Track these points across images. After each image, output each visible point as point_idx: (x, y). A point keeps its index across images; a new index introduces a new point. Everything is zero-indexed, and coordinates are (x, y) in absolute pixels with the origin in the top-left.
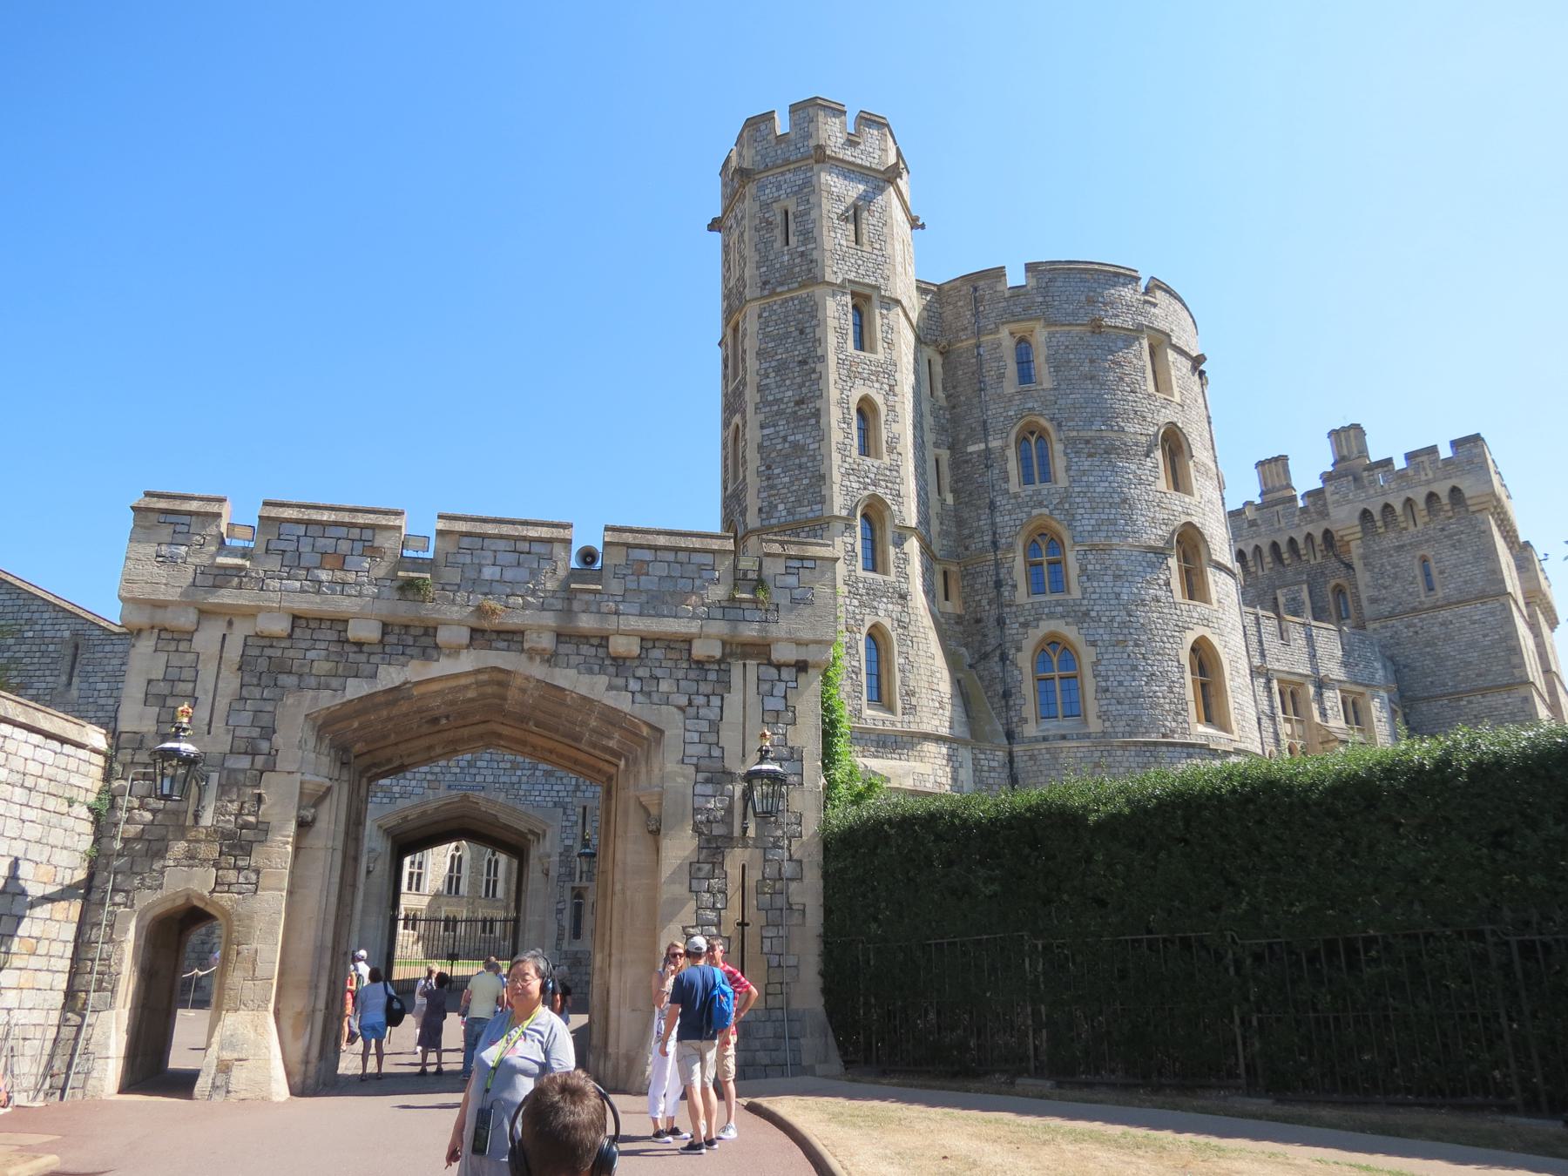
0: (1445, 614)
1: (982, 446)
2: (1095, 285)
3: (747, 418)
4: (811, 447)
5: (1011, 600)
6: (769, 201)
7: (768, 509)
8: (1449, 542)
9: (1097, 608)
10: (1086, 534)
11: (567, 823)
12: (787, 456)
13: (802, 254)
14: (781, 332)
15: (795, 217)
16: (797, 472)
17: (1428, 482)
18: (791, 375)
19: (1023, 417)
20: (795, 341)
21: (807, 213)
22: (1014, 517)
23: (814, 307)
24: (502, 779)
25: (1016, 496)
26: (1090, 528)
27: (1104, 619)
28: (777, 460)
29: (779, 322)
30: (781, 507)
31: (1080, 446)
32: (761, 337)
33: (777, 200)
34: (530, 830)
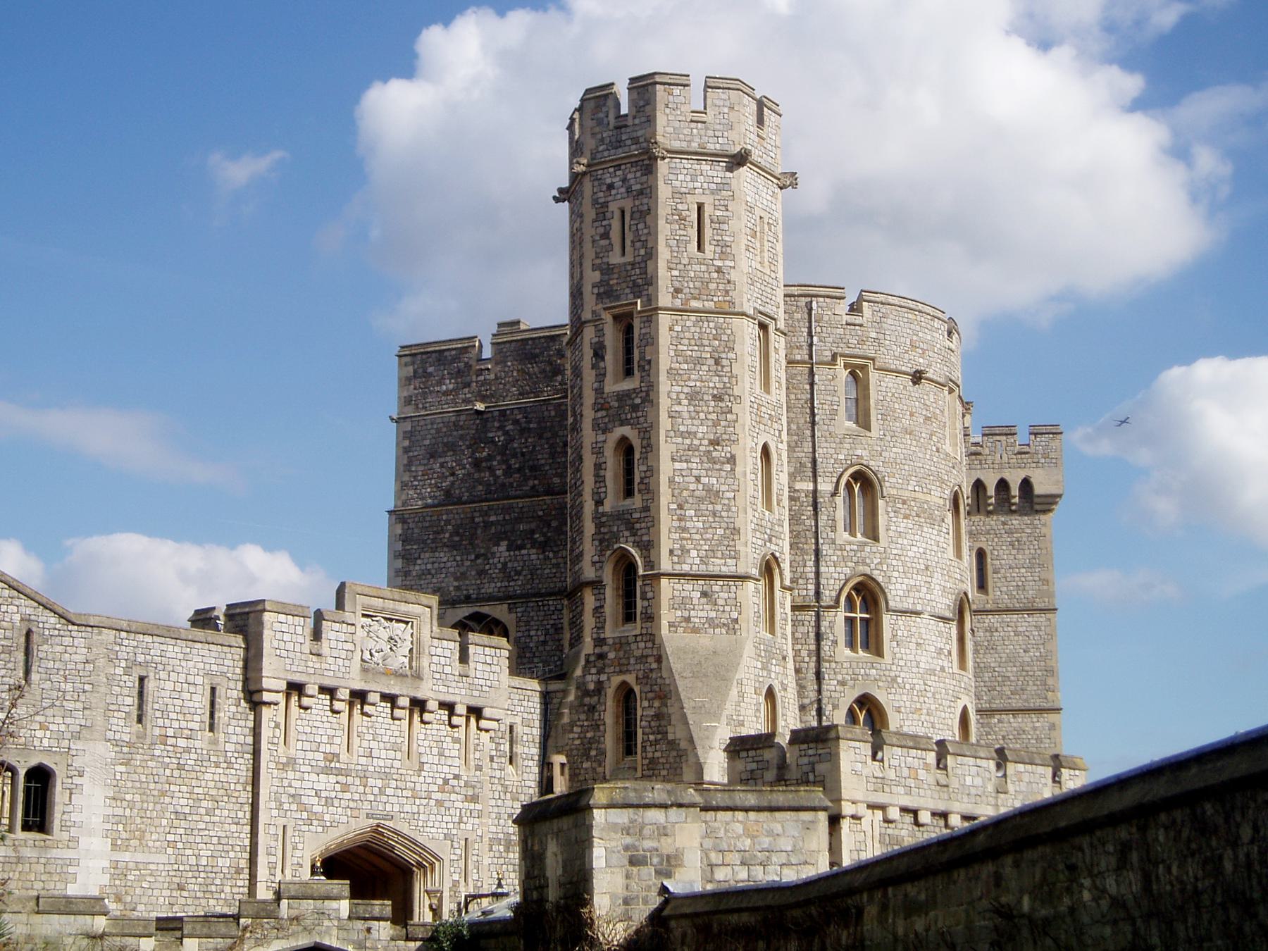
0: (992, 620)
1: (811, 486)
2: (918, 328)
5: (831, 656)
6: (683, 190)
7: (680, 553)
8: (1009, 539)
9: (903, 674)
11: (453, 857)
12: (701, 500)
16: (711, 519)
18: (705, 408)
19: (852, 465)
22: (839, 569)
23: (732, 338)
24: (407, 808)
26: (901, 593)
27: (908, 686)
28: (691, 500)
29: (693, 342)
30: (694, 553)
32: (672, 353)
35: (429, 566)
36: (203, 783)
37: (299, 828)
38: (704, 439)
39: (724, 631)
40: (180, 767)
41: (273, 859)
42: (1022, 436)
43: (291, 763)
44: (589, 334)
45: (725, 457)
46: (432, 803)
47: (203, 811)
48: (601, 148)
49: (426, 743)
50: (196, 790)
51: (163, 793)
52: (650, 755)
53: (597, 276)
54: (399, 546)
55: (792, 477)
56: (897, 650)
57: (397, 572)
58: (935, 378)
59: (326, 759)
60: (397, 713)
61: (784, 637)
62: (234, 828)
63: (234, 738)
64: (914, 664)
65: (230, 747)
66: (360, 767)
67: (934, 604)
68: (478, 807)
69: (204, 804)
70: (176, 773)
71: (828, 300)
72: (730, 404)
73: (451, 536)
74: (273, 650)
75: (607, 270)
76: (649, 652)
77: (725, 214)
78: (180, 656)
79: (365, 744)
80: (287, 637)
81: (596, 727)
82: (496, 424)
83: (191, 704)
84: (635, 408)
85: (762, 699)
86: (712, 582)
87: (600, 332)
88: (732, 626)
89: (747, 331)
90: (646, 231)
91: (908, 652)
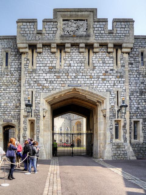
11: (111, 97)
24: (87, 82)
34: (97, 101)
37: (38, 91)
49: (96, 60)
59: (49, 68)
60: (81, 50)
62: (14, 94)
66: (65, 70)
68: (123, 79)
74: (21, 35)
79: (67, 62)
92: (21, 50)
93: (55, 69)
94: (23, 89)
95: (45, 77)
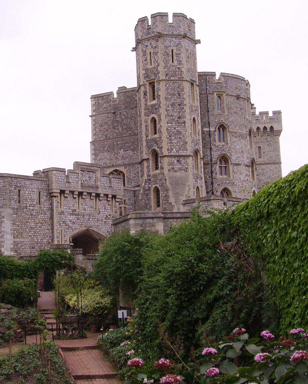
0: (263, 167)
1: (208, 129)
2: (237, 83)
3: (162, 118)
4: (183, 132)
6: (167, 46)
7: (170, 149)
9: (236, 182)
10: (234, 160)
12: (176, 134)
13: (179, 68)
14: (173, 93)
15: (176, 54)
16: (179, 140)
17: (265, 123)
18: (176, 108)
20: (177, 97)
21: (180, 54)
22: (217, 153)
23: (183, 88)
24: (96, 224)
25: (217, 147)
26: (235, 159)
27: (237, 185)
28: (173, 134)
30: (174, 149)
31: (233, 134)
32: (166, 93)
33: (170, 46)
35: (102, 157)
36: (38, 219)
38: (176, 117)
39: (184, 171)
40: (31, 215)
41: (59, 239)
42: (271, 115)
43: (62, 213)
44: (142, 88)
45: (183, 122)
46: (103, 222)
47: (38, 227)
48: (144, 35)
49: (101, 206)
50: (36, 221)
51: (27, 222)
52: (164, 207)
53: (144, 72)
54: (93, 152)
55: (202, 127)
56: (234, 175)
57: (93, 159)
58: (243, 97)
59: (72, 211)
60: (92, 198)
61: (201, 172)
62: (47, 231)
63: (46, 206)
64: (239, 179)
65: (45, 209)
67: (244, 161)
69: (39, 225)
70: (30, 216)
71: (211, 76)
72: (183, 107)
73: (107, 148)
74: (56, 181)
75: (147, 70)
76: (163, 178)
77: (180, 52)
78: (30, 184)
79: (83, 207)
80: (59, 178)
81: (149, 200)
82: (119, 116)
83: (33, 197)
84: (156, 109)
85: (195, 190)
86: (180, 158)
87: (145, 88)
88: (186, 170)
89: (187, 86)
90: (157, 58)
91: (237, 175)
92: (54, 194)
93: (76, 212)
94: (55, 228)
95: (70, 219)
